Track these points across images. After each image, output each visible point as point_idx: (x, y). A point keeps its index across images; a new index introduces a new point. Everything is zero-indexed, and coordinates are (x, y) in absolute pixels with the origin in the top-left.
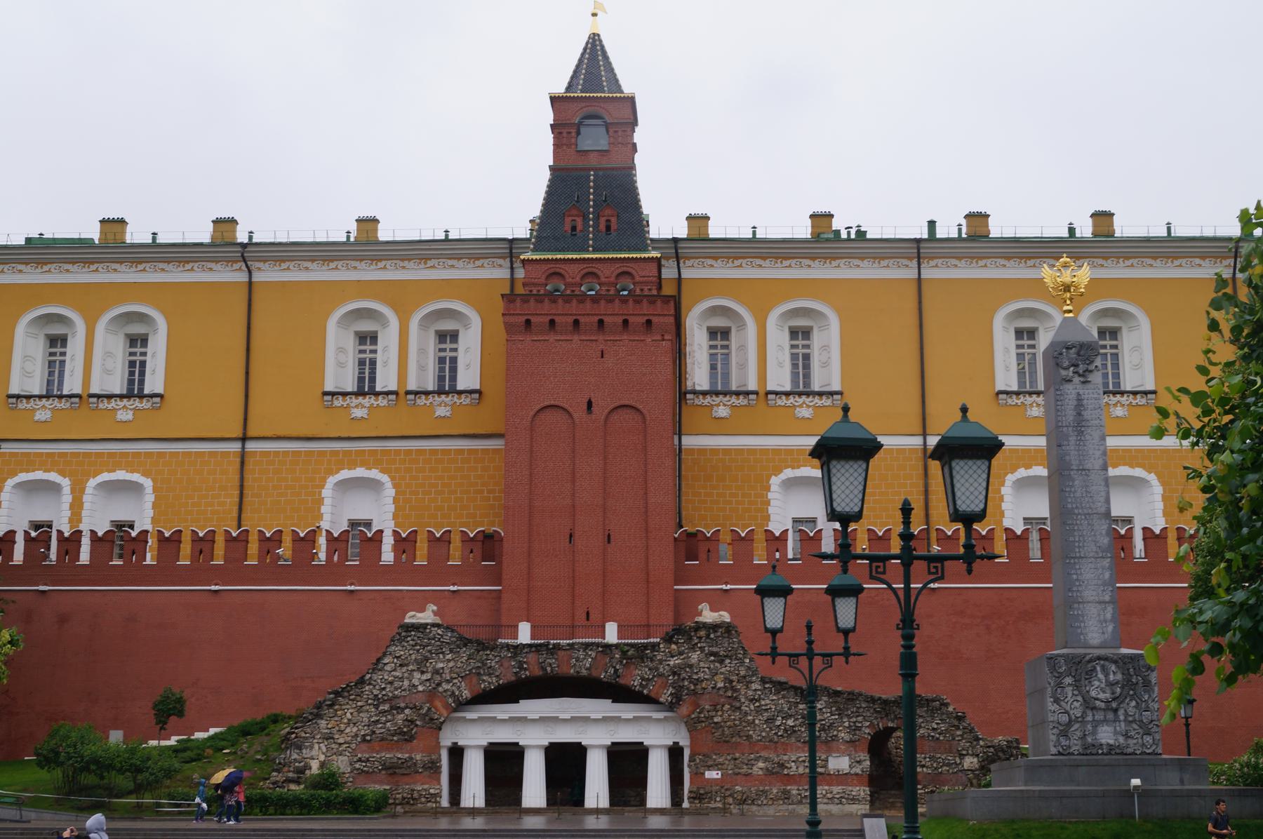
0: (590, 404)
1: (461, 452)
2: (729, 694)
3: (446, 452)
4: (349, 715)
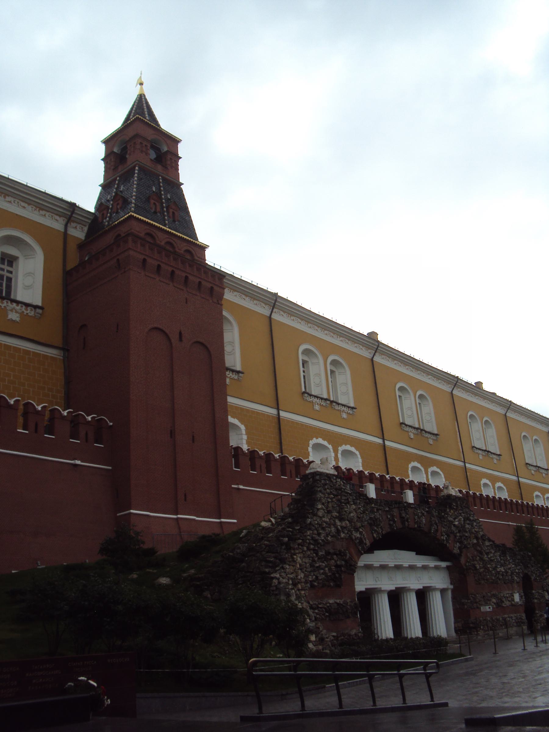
0: (180, 334)
1: (27, 352)
2: (479, 548)
3: (17, 349)
4: (299, 559)
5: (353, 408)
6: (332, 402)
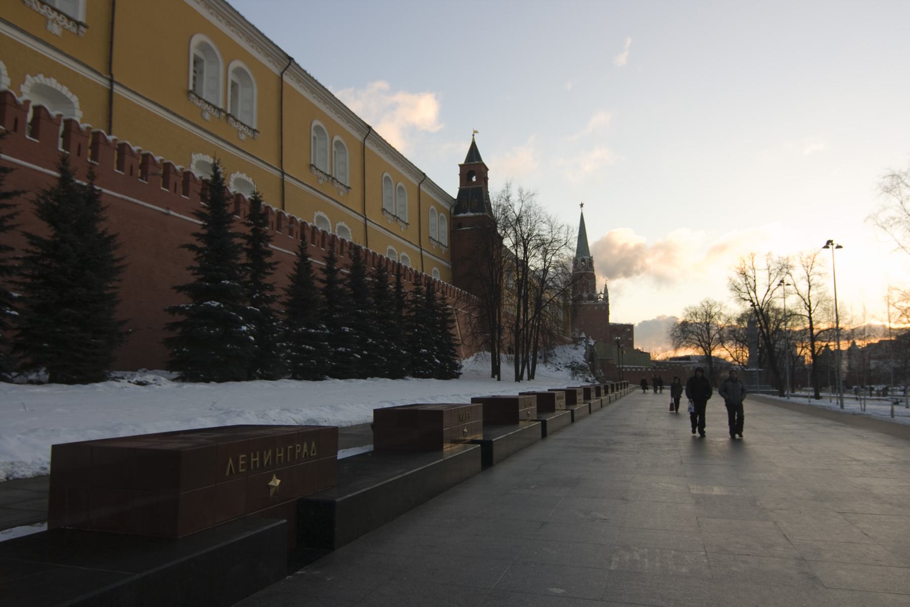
5: (254, 131)
6: (228, 115)
